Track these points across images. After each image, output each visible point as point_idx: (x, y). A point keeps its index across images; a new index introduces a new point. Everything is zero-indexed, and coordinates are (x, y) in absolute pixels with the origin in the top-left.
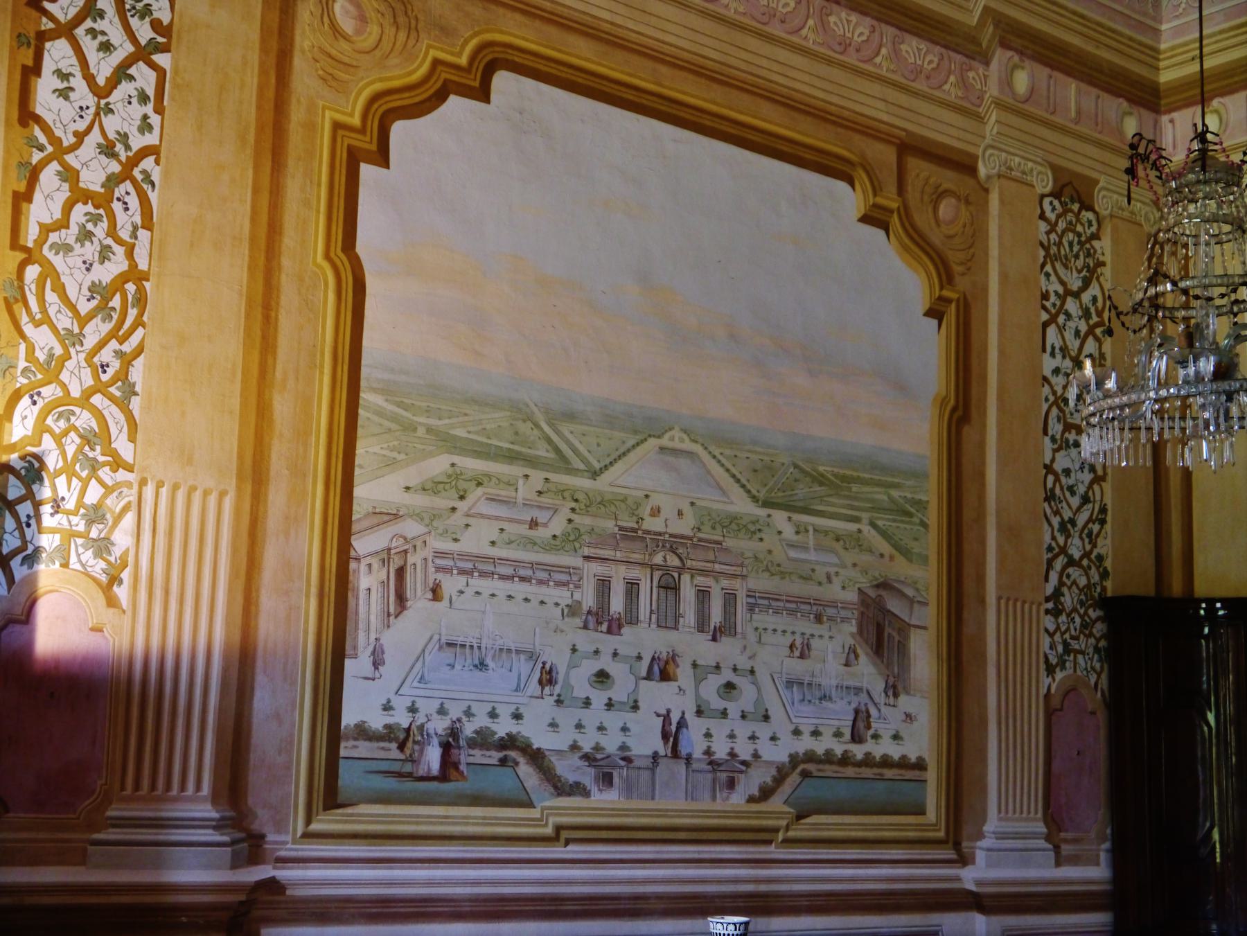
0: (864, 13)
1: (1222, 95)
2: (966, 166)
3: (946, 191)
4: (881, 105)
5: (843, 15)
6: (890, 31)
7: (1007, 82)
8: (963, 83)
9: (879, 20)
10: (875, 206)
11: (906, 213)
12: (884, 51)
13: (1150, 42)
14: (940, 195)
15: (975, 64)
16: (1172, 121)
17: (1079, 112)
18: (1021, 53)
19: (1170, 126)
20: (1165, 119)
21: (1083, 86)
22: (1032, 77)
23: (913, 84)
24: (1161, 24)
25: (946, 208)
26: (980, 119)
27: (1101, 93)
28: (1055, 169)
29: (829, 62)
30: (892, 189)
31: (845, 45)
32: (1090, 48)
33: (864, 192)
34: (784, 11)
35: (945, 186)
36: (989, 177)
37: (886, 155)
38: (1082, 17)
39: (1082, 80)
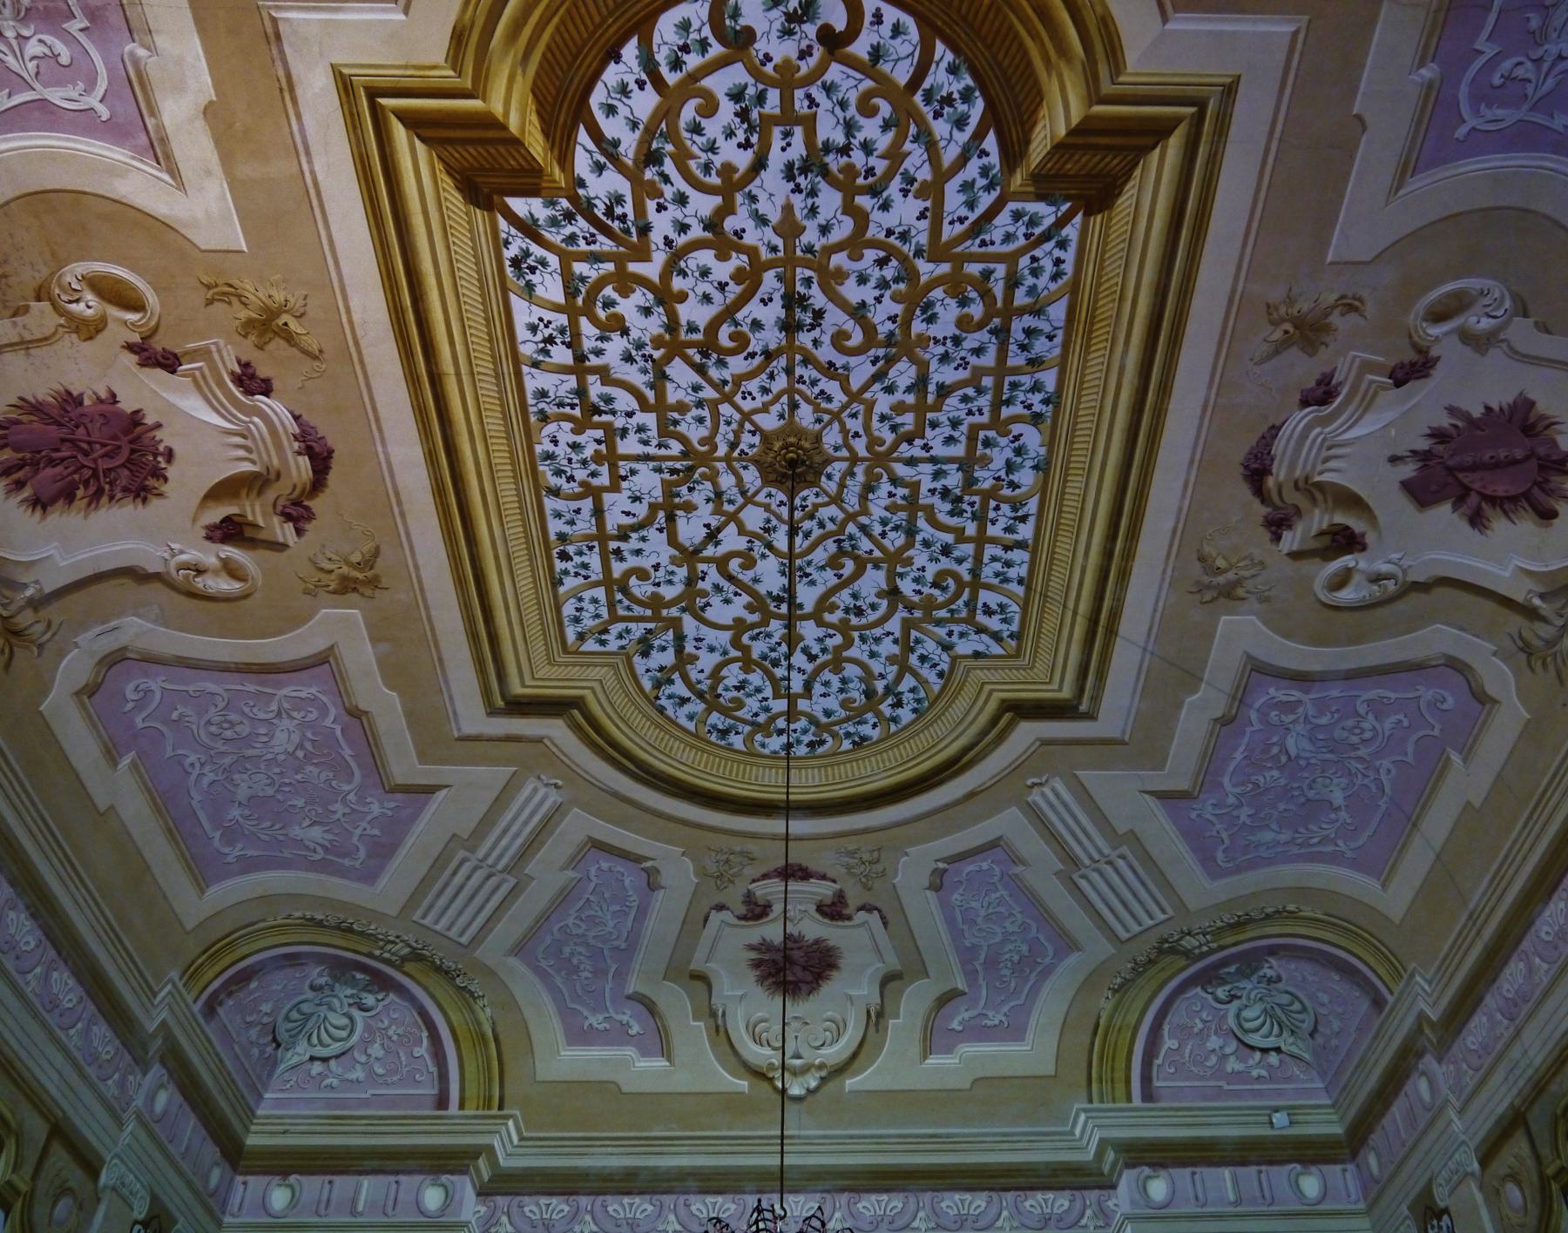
0: (80, 982)
1: (301, 1173)
2: (91, 1167)
3: (69, 1189)
4: (55, 1076)
5: (65, 975)
6: (92, 1007)
7: (151, 1098)
8: (122, 1085)
9: (88, 993)
10: (9, 1183)
11: (30, 1198)
12: (79, 1025)
13: (252, 1103)
14: (65, 1191)
15: (137, 1069)
16: (245, 1183)
17: (187, 1149)
18: (170, 1073)
19: (241, 1188)
20: (240, 1179)
21: (199, 1124)
22: (170, 1101)
23: (86, 1068)
24: (266, 1091)
25: (63, 1207)
26: (120, 1124)
27: (208, 1139)
28: (155, 1199)
29: (36, 1015)
30: (27, 1170)
31: (54, 1005)
32: (215, 1091)
33: (7, 1164)
34: (24, 948)
35: (72, 1184)
36: (105, 1187)
37: (37, 1129)
38: (221, 1061)
39: (200, 1120)
